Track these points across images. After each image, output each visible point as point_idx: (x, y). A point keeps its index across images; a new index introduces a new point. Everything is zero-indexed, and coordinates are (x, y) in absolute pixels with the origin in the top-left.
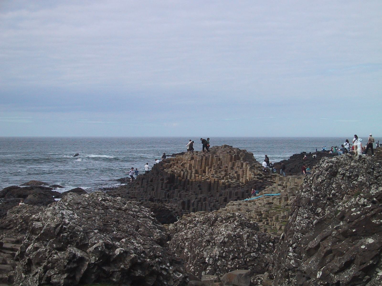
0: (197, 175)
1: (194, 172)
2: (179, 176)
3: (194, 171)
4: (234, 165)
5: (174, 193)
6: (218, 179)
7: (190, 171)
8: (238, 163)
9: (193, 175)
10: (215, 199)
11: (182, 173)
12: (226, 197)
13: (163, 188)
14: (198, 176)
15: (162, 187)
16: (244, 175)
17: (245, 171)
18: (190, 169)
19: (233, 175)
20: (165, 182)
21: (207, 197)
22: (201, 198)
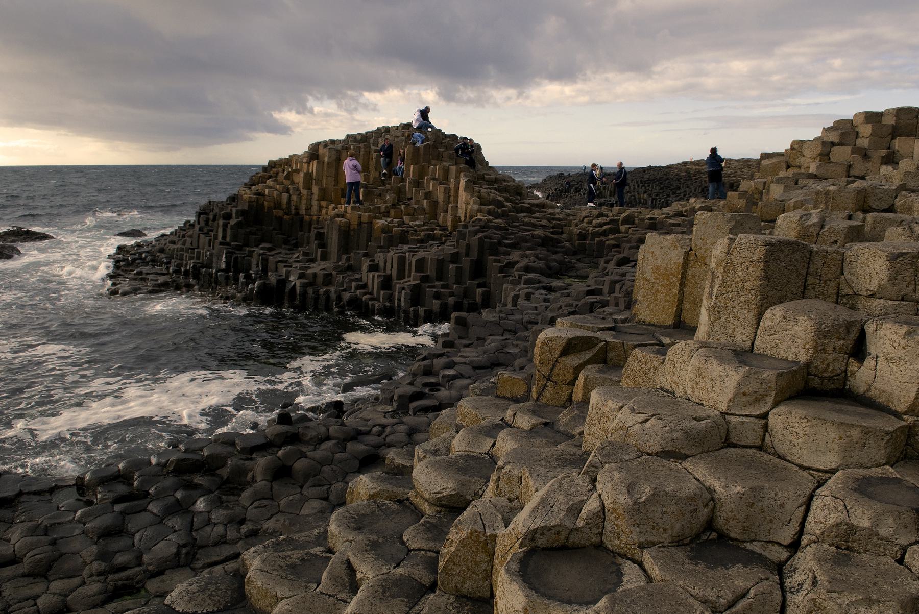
0: (324, 203)
1: (315, 197)
2: (278, 205)
3: (315, 189)
4: (421, 173)
5: (250, 254)
6: (369, 216)
7: (304, 192)
8: (436, 170)
9: (315, 203)
10: (357, 280)
11: (285, 196)
12: (388, 272)
13: (228, 239)
14: (327, 208)
15: (224, 237)
16: (449, 202)
17: (452, 193)
18: (308, 185)
19: (418, 202)
20: (233, 222)
21: (334, 273)
22: (315, 275)
